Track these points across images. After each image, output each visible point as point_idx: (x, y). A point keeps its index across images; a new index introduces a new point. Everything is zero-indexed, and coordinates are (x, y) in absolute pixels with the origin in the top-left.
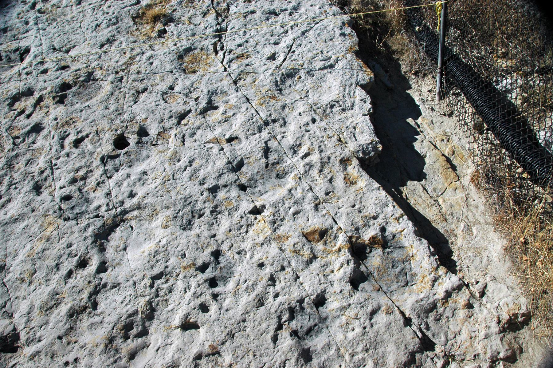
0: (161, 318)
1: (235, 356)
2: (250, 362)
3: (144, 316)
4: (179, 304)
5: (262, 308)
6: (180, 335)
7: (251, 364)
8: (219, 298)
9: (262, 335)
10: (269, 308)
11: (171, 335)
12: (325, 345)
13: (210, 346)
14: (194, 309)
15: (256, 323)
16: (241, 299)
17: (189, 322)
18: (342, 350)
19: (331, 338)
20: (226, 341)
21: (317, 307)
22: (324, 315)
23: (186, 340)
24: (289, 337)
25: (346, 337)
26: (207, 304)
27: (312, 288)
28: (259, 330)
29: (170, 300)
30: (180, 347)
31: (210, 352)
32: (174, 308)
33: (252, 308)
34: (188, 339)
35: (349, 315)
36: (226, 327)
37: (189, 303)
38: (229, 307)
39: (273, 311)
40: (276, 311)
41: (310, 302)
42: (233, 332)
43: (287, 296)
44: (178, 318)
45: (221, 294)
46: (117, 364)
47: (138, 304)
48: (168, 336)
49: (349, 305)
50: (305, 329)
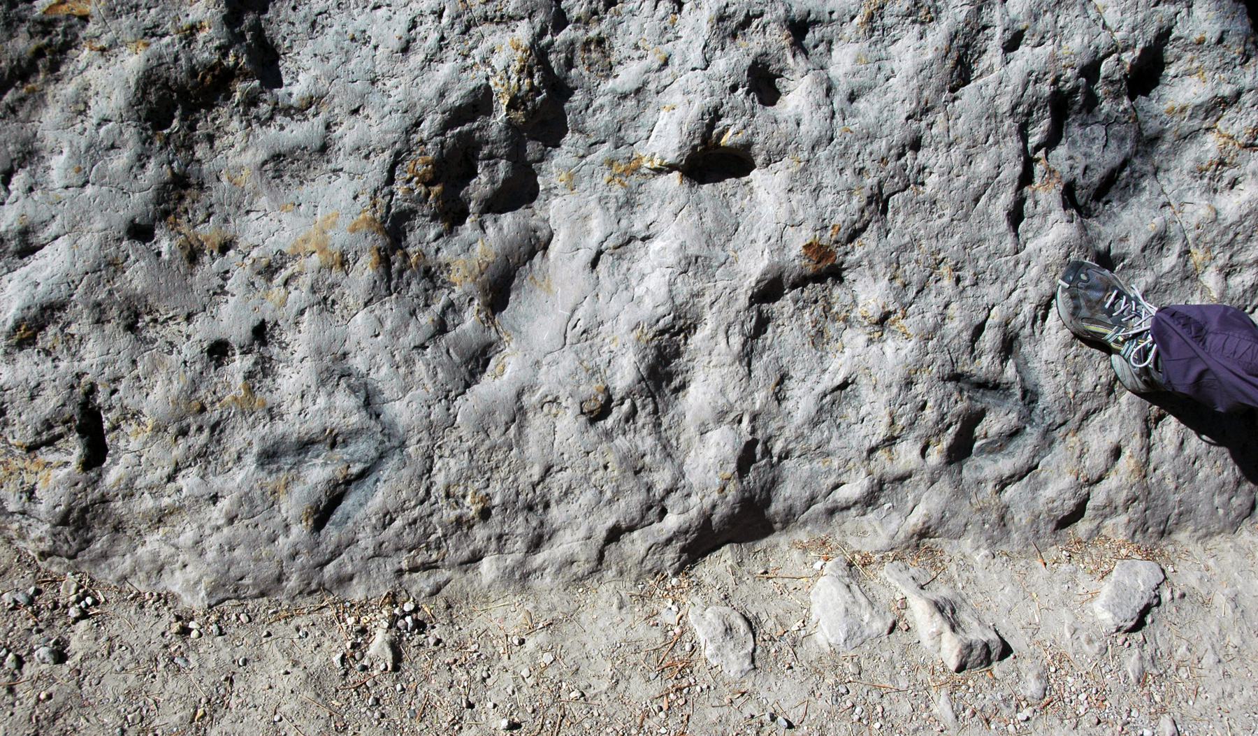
0: (590, 123)
1: (897, 283)
2: (946, 307)
3: (519, 116)
4: (666, 63)
5: (968, 92)
6: (683, 199)
7: (950, 311)
8: (810, 38)
9: (977, 200)
10: (990, 91)
11: (643, 198)
12: (1153, 238)
13: (807, 247)
14: (734, 88)
15: (956, 154)
16: (891, 49)
17: (717, 145)
18: (1198, 255)
19: (1168, 212)
20: (864, 229)
21: (1132, 98)
22: (1152, 126)
23: (708, 219)
24: (1058, 213)
25: (1217, 214)
26: (774, 67)
27: (1129, 19)
28: (968, 182)
29: (617, 43)
30: (692, 250)
31: (810, 270)
32: (645, 83)
33: (940, 91)
34: (717, 219)
35: (1231, 132)
36: (860, 172)
37: (707, 64)
38: (857, 81)
39: (1004, 104)
40: (1014, 108)
41: (1117, 76)
42: (886, 191)
43: (1048, 47)
44: (673, 129)
45: (816, 22)
46: (452, 334)
47: (485, 61)
48: (629, 204)
49: (1239, 94)
50: (1096, 178)
